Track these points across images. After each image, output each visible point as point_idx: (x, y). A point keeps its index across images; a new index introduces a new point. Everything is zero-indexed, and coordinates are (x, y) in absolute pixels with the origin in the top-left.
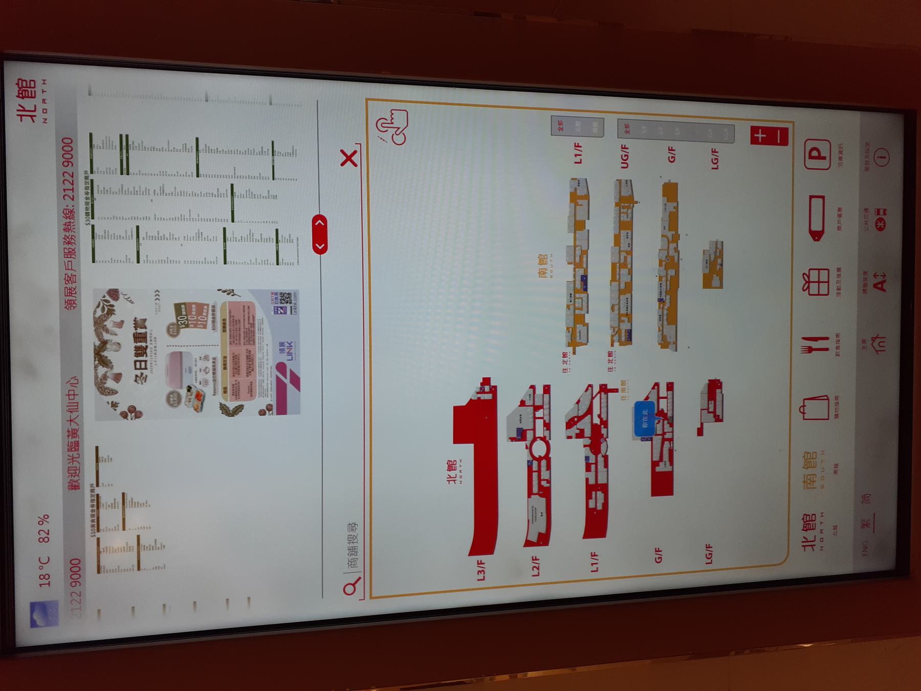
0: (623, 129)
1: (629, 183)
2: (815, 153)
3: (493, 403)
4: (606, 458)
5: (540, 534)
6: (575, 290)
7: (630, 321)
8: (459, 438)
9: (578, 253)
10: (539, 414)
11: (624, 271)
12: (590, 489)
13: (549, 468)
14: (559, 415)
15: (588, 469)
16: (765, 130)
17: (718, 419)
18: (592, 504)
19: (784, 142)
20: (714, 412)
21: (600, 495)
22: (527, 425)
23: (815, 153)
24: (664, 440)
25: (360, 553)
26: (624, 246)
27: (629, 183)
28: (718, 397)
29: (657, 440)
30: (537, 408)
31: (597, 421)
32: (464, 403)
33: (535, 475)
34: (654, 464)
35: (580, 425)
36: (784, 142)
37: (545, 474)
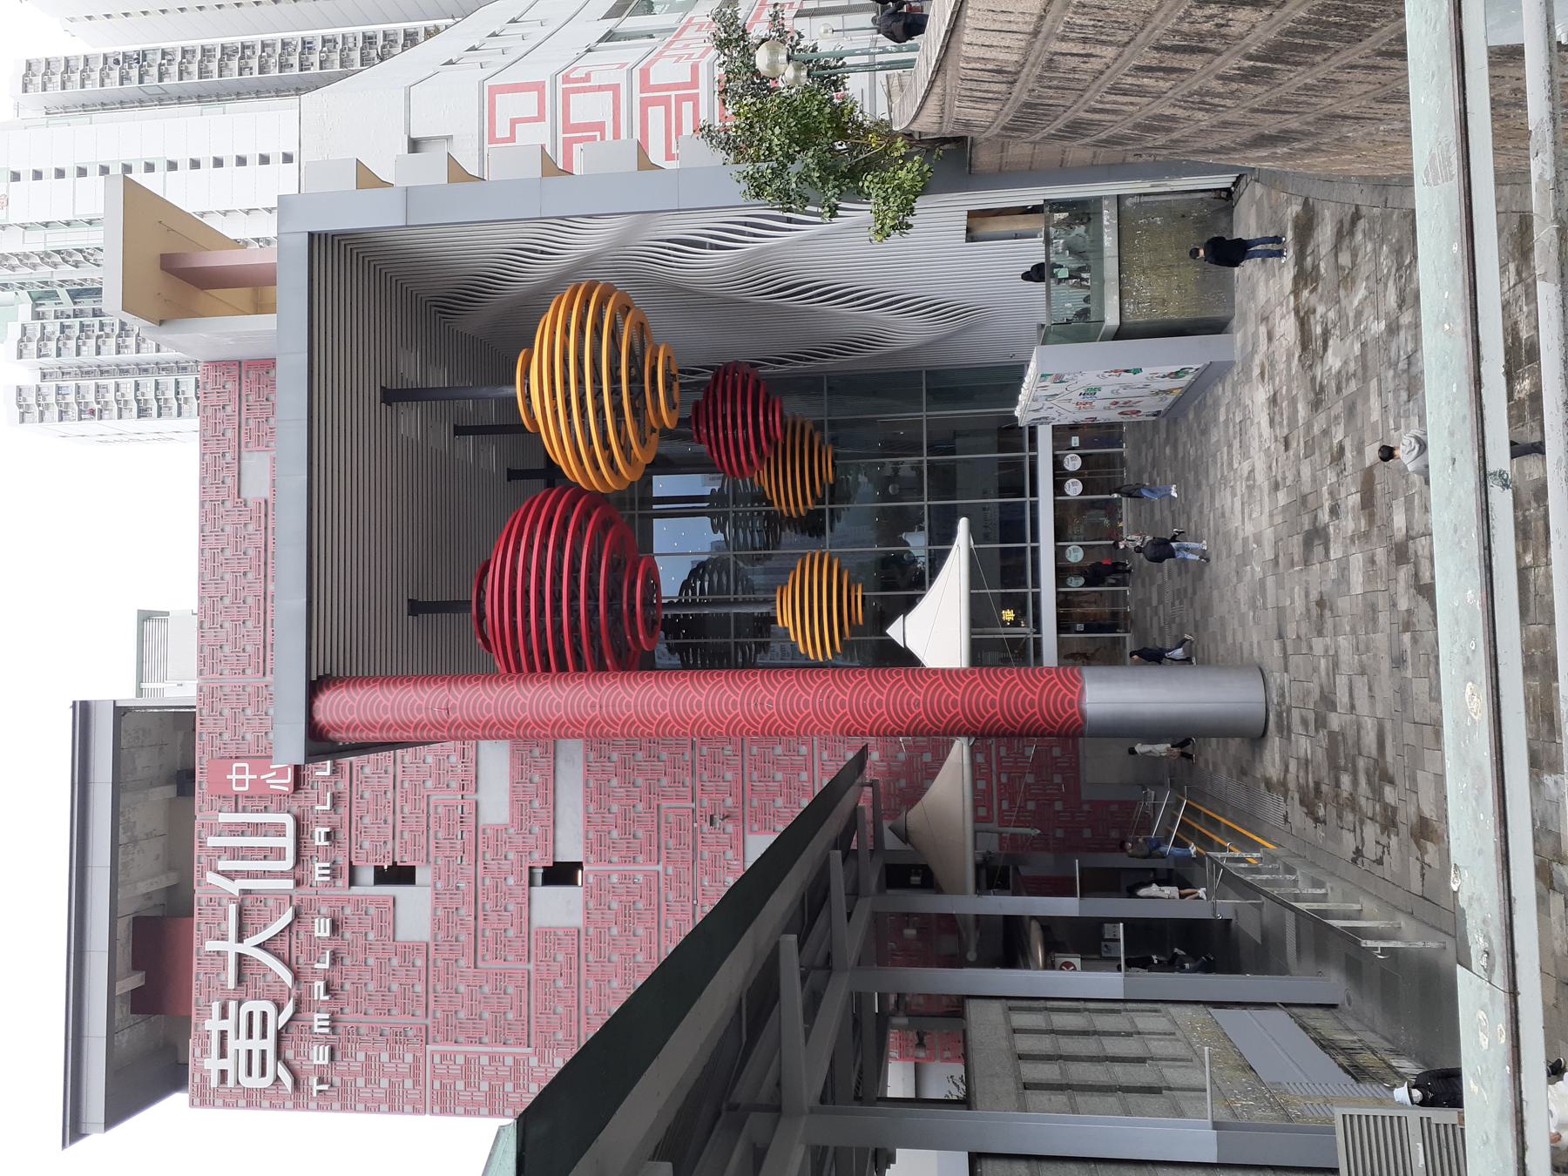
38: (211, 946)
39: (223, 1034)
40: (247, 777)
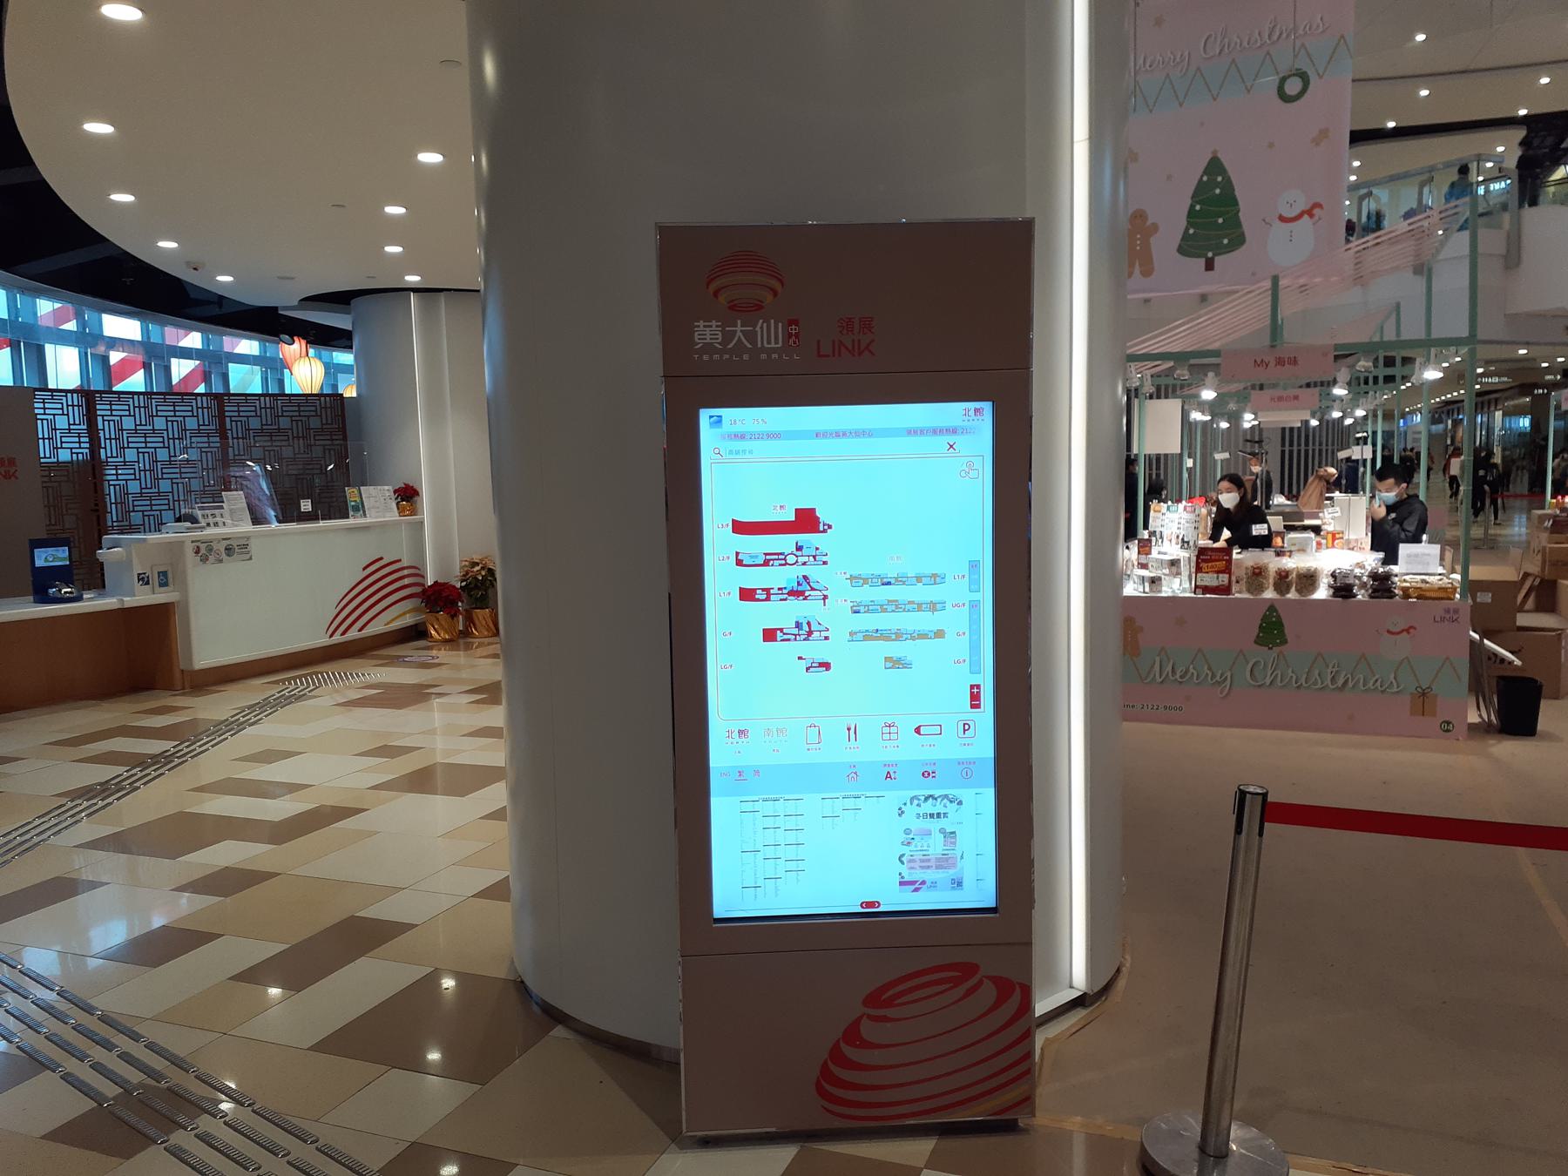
0: (974, 603)
1: (944, 609)
2: (967, 727)
3: (817, 531)
4: (785, 600)
5: (742, 561)
6: (882, 578)
7: (865, 612)
8: (797, 511)
9: (904, 579)
10: (811, 558)
11: (893, 608)
12: (767, 591)
13: (780, 565)
14: (813, 572)
15: (779, 589)
16: (979, 693)
17: (807, 669)
18: (758, 592)
19: (973, 707)
20: (811, 667)
21: (764, 597)
22: (805, 551)
23: (967, 727)
24: (795, 635)
25: (737, 456)
26: (908, 607)
27: (944, 609)
28: (821, 669)
29: (795, 631)
30: (814, 557)
31: (807, 594)
32: (818, 514)
33: (776, 557)
34: (781, 630)
35: (805, 584)
36: (973, 707)
37: (777, 563)
38: (739, 322)
39: (711, 326)
40: (794, 332)
